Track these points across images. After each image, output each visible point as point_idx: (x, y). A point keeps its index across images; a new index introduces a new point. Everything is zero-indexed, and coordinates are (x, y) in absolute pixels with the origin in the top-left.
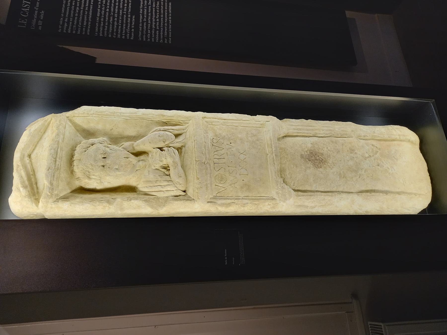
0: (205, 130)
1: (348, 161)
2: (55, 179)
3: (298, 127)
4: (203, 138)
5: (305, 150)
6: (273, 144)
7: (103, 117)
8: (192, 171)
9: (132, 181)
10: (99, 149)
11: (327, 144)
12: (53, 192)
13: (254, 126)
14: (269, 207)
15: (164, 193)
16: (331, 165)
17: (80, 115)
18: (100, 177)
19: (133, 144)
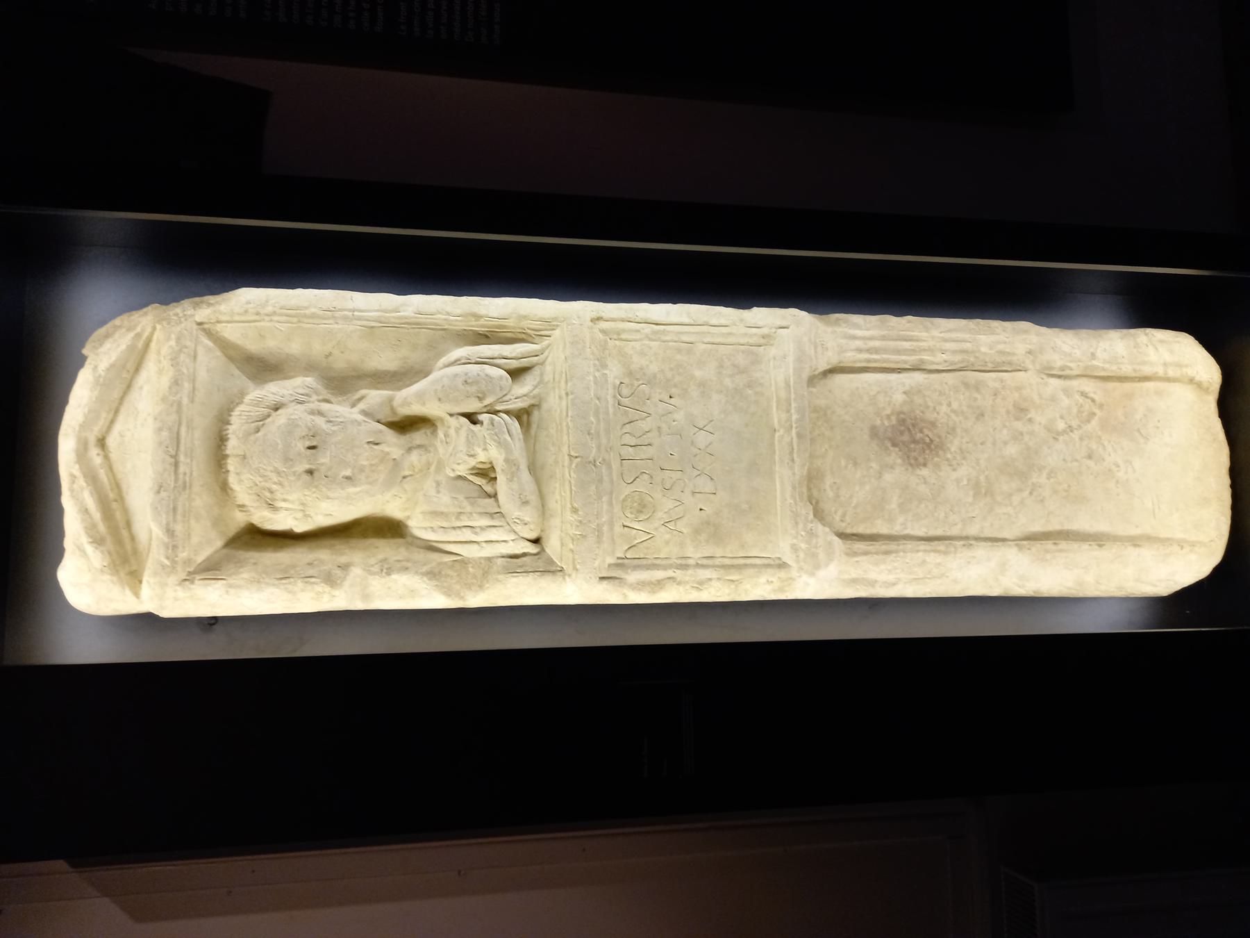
0: (598, 360)
1: (1006, 443)
2: (179, 517)
4: (593, 384)
6: (795, 399)
7: (303, 323)
8: (557, 485)
9: (391, 506)
10: (297, 426)
11: (952, 393)
12: (177, 556)
13: (742, 341)
14: (769, 587)
15: (479, 548)
16: (955, 458)
17: (237, 318)
18: (303, 504)
19: (391, 400)
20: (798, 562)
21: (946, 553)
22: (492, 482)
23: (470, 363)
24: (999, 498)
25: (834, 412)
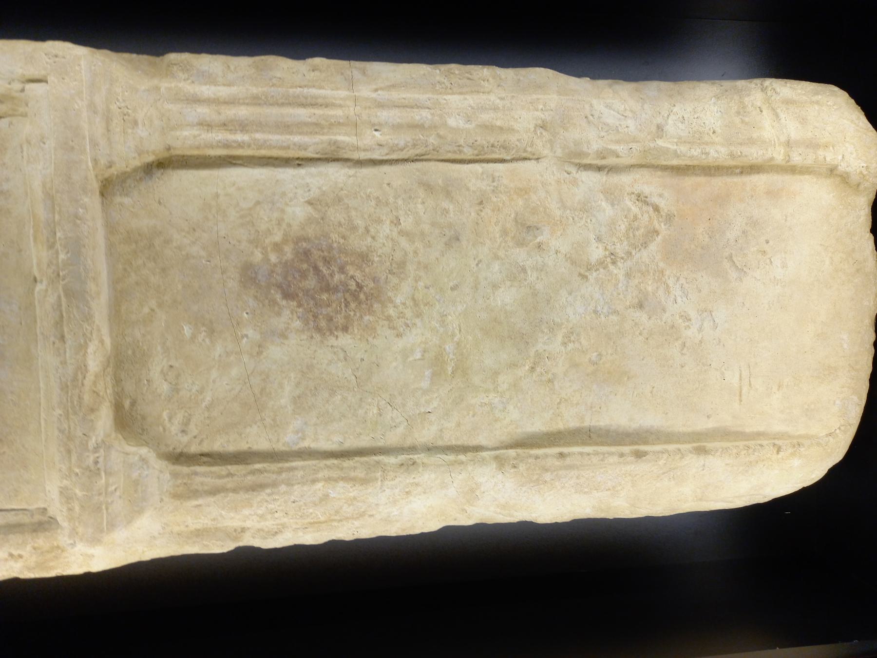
1: (495, 286)
3: (230, 112)
5: (267, 241)
11: (400, 202)
16: (401, 315)
20: (70, 519)
21: (365, 482)
24: (476, 380)
25: (167, 242)
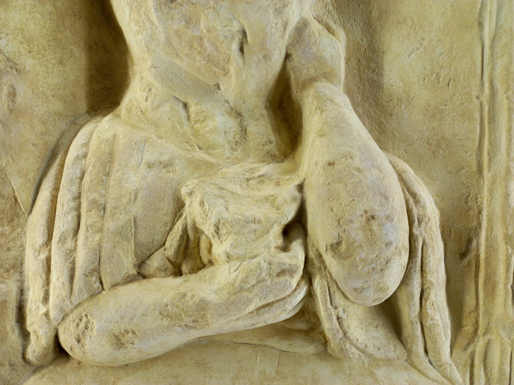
22: (170, 265)
23: (411, 224)
